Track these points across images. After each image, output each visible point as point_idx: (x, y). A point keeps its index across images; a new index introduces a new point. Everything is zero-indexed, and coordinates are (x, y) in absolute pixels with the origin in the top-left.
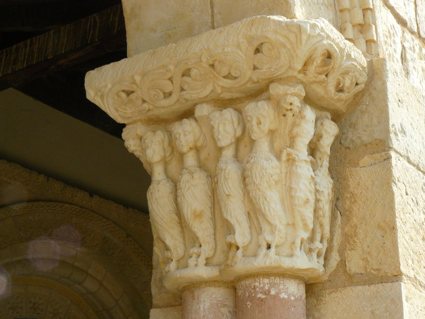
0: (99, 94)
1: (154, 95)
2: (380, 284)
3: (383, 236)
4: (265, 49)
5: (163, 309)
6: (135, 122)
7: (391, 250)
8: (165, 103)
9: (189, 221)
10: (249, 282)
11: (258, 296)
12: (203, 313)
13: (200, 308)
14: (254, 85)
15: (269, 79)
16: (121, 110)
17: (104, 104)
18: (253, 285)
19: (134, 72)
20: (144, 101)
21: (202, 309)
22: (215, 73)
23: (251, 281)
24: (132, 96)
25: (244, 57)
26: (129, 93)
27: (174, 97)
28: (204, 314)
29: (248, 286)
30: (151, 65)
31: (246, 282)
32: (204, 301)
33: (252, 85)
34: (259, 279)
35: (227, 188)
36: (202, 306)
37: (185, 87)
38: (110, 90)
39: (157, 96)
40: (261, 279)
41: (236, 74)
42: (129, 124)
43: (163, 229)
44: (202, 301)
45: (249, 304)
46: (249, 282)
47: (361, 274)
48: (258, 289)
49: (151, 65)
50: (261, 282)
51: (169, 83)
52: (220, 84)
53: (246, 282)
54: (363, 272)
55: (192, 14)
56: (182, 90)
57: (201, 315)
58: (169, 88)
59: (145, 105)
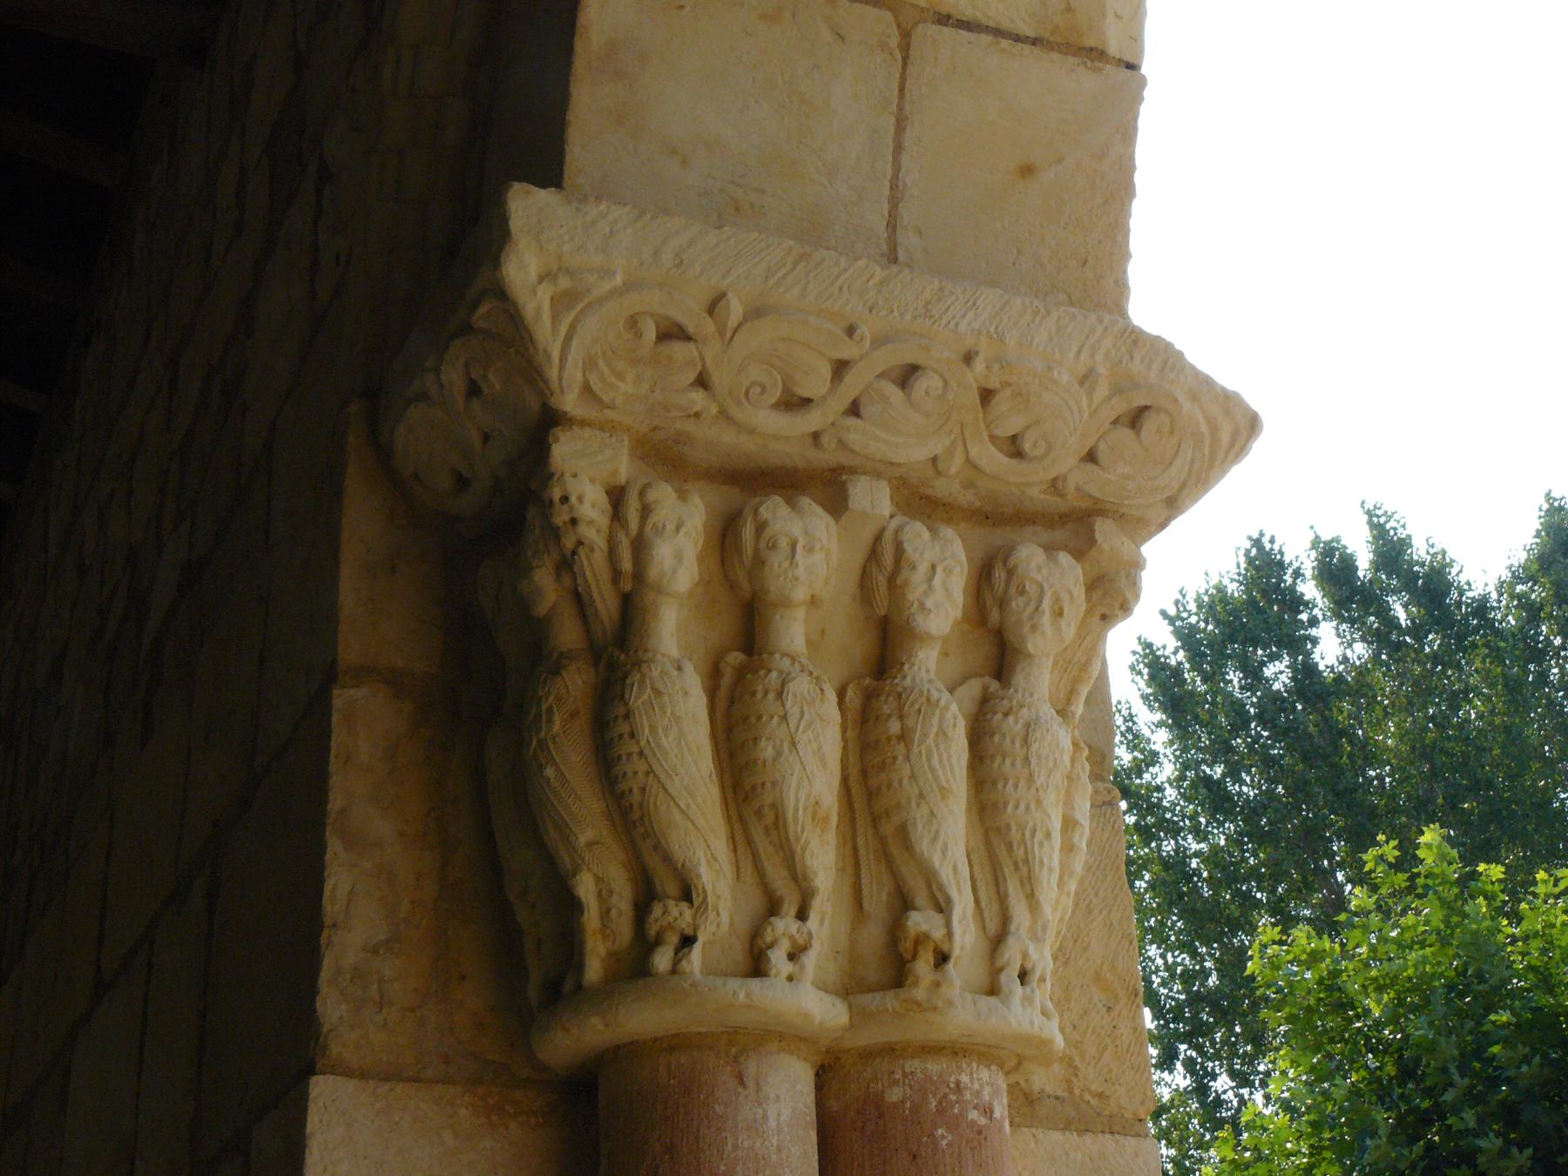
0: (564, 283)
1: (755, 383)
2: (1108, 1136)
3: (1110, 1008)
4: (1150, 424)
5: (372, 1083)
6: (611, 428)
7: (1131, 1049)
8: (768, 420)
9: (799, 832)
10: (939, 1068)
11: (970, 1117)
12: (776, 1137)
13: (765, 1117)
14: (1048, 497)
15: (1096, 500)
16: (606, 371)
17: (555, 319)
18: (953, 1079)
19: (728, 281)
20: (702, 382)
21: (772, 1124)
22: (981, 415)
23: (945, 1066)
24: (678, 349)
25: (1086, 415)
26: (672, 333)
27: (812, 420)
28: (778, 1140)
29: (935, 1078)
30: (796, 291)
31: (929, 1066)
32: (778, 1097)
33: (1042, 496)
34: (969, 1065)
35: (943, 766)
36: (772, 1114)
37: (867, 410)
38: (614, 293)
39: (758, 390)
40: (974, 1065)
41: (1035, 444)
42: (583, 423)
43: (691, 826)
44: (772, 1096)
45: (943, 1137)
46: (939, 1068)
47: (1057, 1098)
48: (968, 1093)
49: (796, 291)
50: (975, 1076)
51: (826, 371)
52: (974, 452)
53: (929, 1066)
54: (1060, 1093)
55: (826, 182)
56: (854, 410)
57: (770, 1141)
58: (815, 383)
59: (698, 398)
